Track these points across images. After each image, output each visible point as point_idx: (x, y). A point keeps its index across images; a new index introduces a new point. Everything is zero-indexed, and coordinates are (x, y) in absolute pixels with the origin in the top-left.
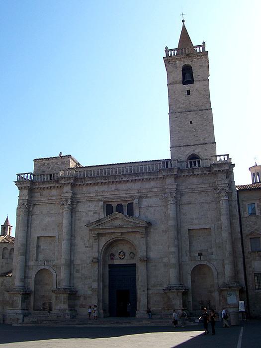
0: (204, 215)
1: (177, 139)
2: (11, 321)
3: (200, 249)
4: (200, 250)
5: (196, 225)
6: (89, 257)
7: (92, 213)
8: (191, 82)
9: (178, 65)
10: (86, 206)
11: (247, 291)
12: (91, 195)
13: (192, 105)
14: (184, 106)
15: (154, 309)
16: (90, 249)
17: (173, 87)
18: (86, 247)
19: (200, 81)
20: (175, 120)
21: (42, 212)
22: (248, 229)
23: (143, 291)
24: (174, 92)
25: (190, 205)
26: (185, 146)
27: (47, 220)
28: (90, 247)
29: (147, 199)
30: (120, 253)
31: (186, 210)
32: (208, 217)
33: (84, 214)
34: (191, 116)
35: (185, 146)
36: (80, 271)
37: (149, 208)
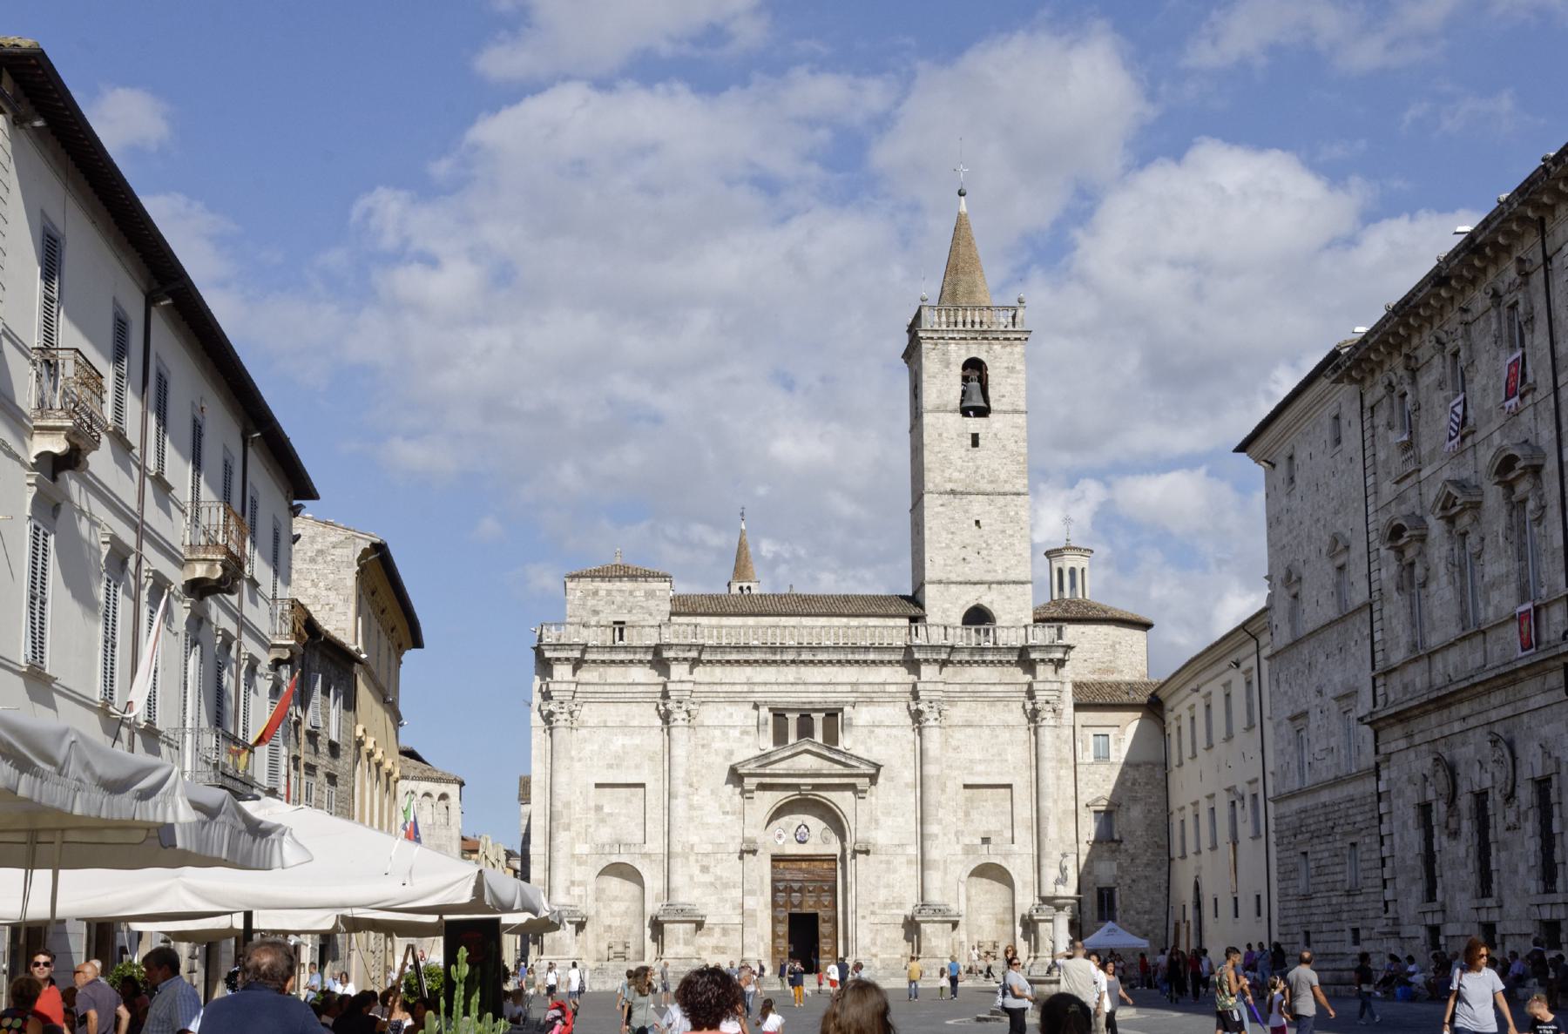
0: (1000, 755)
1: (942, 562)
5: (980, 774)
6: (733, 838)
7: (735, 733)
8: (983, 412)
9: (954, 355)
10: (722, 713)
11: (1080, 926)
12: (738, 688)
13: (983, 477)
14: (963, 476)
15: (885, 956)
16: (734, 817)
17: (938, 418)
18: (724, 813)
19: (1005, 412)
20: (938, 513)
21: (605, 722)
22: (1091, 790)
23: (864, 917)
24: (940, 435)
25: (969, 731)
26: (961, 583)
27: (619, 741)
28: (734, 813)
29: (872, 708)
30: (800, 827)
31: (959, 740)
32: (1006, 761)
33: (717, 733)
34: (978, 506)
35: (961, 583)
37: (876, 730)
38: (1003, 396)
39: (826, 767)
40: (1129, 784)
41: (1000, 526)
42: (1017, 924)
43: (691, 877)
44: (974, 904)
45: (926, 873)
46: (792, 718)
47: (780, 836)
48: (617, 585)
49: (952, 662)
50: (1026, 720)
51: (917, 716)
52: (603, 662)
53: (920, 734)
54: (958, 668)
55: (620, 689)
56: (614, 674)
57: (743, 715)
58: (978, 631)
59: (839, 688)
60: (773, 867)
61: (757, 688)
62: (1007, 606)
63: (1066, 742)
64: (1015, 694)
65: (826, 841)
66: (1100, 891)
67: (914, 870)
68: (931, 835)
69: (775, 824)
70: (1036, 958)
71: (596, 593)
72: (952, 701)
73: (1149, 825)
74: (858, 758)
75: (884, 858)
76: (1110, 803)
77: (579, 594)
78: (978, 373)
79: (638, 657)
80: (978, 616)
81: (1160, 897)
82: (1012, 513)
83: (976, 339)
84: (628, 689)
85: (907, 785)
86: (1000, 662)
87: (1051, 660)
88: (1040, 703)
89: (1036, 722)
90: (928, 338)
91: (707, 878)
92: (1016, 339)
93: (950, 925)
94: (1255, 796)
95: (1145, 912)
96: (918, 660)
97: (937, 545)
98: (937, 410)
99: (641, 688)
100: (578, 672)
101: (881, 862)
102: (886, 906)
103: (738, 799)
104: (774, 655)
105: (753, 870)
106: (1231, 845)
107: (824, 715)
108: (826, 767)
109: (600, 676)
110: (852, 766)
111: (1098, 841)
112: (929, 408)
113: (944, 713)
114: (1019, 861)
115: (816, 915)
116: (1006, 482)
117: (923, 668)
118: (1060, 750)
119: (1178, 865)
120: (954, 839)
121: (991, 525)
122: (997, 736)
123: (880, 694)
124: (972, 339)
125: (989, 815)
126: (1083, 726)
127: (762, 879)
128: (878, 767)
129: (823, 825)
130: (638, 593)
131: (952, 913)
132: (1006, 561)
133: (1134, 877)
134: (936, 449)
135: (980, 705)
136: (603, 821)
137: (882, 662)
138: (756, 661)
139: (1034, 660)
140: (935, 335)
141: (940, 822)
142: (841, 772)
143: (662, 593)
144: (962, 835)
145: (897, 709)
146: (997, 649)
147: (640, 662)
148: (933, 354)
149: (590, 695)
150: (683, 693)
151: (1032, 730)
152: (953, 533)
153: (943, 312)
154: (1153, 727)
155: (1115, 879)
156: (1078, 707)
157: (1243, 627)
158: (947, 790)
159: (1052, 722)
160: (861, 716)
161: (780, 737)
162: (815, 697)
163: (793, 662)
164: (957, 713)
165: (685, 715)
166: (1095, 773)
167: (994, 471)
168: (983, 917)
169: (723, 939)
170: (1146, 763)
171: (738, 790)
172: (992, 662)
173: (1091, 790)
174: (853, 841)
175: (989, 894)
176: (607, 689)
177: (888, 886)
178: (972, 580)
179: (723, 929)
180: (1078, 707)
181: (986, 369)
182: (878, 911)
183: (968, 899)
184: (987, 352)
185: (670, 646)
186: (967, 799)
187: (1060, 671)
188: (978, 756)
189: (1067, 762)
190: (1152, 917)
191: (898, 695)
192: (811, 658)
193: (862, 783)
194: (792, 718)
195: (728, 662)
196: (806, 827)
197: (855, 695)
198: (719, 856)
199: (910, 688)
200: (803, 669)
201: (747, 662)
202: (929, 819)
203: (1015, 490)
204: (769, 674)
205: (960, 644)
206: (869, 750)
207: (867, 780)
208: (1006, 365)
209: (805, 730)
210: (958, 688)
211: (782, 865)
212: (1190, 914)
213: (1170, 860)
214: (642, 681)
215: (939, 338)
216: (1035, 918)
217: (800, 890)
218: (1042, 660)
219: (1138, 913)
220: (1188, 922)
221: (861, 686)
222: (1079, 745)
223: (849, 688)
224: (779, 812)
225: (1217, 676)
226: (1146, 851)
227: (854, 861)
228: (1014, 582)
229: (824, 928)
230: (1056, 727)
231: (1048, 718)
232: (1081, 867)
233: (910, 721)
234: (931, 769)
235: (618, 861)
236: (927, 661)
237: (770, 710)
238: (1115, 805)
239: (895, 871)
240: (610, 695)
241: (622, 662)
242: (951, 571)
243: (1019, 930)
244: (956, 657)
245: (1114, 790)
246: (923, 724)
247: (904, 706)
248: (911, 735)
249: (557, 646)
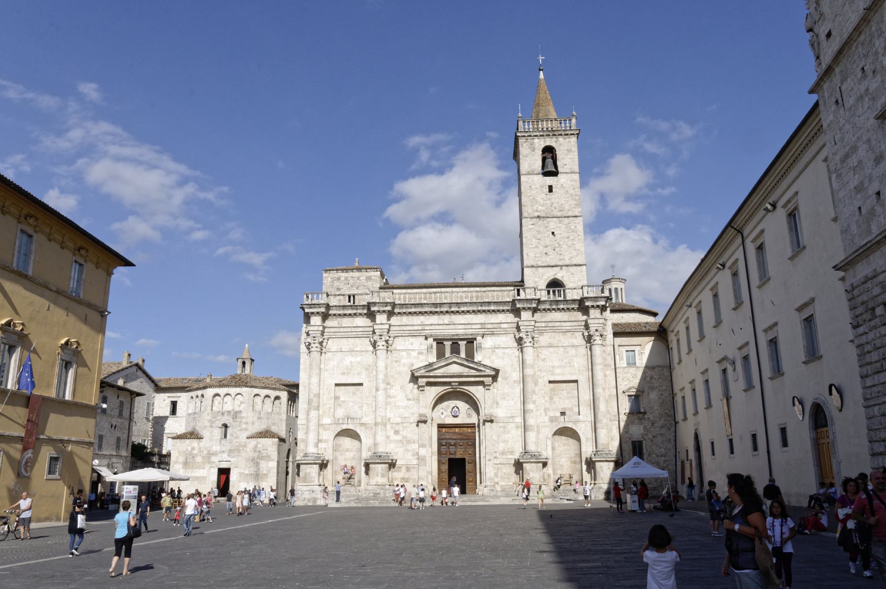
0: (570, 363)
1: (534, 255)
2: (306, 502)
3: (563, 407)
4: (562, 409)
5: (558, 375)
6: (413, 414)
7: (415, 354)
8: (555, 174)
9: (537, 145)
10: (407, 342)
12: (416, 328)
13: (555, 208)
14: (544, 208)
15: (503, 483)
16: (414, 402)
17: (529, 178)
18: (408, 400)
19: (567, 173)
20: (530, 229)
21: (341, 349)
22: (626, 383)
23: (490, 460)
24: (530, 187)
25: (551, 349)
26: (544, 267)
27: (349, 360)
28: (414, 400)
29: (494, 338)
32: (574, 366)
33: (404, 353)
34: (553, 224)
35: (544, 267)
36: (400, 433)
37: (497, 350)
38: (566, 165)
39: (466, 371)
40: (648, 379)
41: (567, 235)
42: (583, 463)
43: (388, 437)
44: (557, 452)
45: (526, 433)
46: (448, 344)
47: (442, 413)
48: (351, 274)
49: (539, 310)
50: (585, 342)
51: (520, 341)
52: (340, 315)
53: (522, 351)
54: (544, 313)
55: (349, 330)
56: (346, 322)
57: (420, 344)
58: (554, 292)
59: (474, 327)
60: (439, 431)
61: (426, 328)
62: (572, 279)
63: (609, 354)
64: (578, 327)
65: (469, 416)
66: (633, 443)
67: (520, 432)
68: (528, 410)
69: (440, 406)
70: (595, 484)
71: (339, 279)
72: (541, 333)
73: (662, 403)
74: (484, 366)
75: (501, 425)
76: (638, 391)
77: (329, 279)
78: (551, 155)
79: (359, 311)
80: (555, 284)
81: (671, 446)
82: (573, 227)
83: (549, 135)
84: (353, 330)
85: (515, 382)
86: (568, 309)
87: (598, 306)
88: (592, 331)
89: (590, 343)
90: (522, 136)
91: (398, 438)
92: (571, 134)
93: (541, 465)
94: (746, 358)
95: (662, 456)
96: (519, 308)
97: (531, 246)
98: (529, 174)
99: (360, 329)
100: (326, 322)
101: (500, 427)
102: (503, 453)
103: (416, 391)
104: (436, 309)
105: (424, 433)
106: (725, 400)
107: (465, 342)
108: (466, 371)
109: (338, 323)
110: (481, 371)
111: (631, 414)
112: (524, 173)
113: (535, 339)
114: (583, 425)
115: (464, 459)
116: (569, 210)
117: (522, 313)
118: (606, 360)
119: (682, 425)
120: (542, 411)
121: (561, 234)
122: (568, 352)
123: (498, 330)
124: (547, 135)
125: (565, 398)
126: (619, 346)
127: (431, 438)
128: (497, 371)
129: (468, 406)
130: (362, 278)
131: (542, 457)
132: (570, 253)
133: (654, 434)
134: (530, 194)
135: (557, 334)
136: (340, 405)
137: (499, 311)
138: (426, 312)
139: (588, 306)
140: (526, 134)
141: (534, 402)
142: (474, 374)
143: (375, 278)
144: (549, 411)
145: (508, 338)
146: (565, 301)
147: (360, 314)
148: (525, 145)
149: (332, 334)
150: (383, 330)
151: (588, 348)
152: (539, 239)
153: (531, 123)
154: (661, 345)
155: (643, 435)
156: (616, 334)
157: (730, 225)
158: (539, 384)
159: (600, 342)
160: (487, 343)
161: (440, 355)
162: (460, 331)
163: (447, 312)
164: (544, 339)
165: (384, 343)
166: (627, 373)
167: (561, 205)
168: (563, 459)
169: (407, 473)
170: (660, 366)
171: (416, 386)
172: (563, 309)
173: (626, 383)
174: (483, 415)
175: (565, 445)
176: (342, 330)
177: (504, 441)
178: (551, 265)
179: (407, 467)
180: (616, 334)
181: (555, 151)
182: (499, 456)
183: (553, 449)
184: (556, 142)
185: (375, 304)
186: (551, 390)
187: (604, 313)
188: (556, 364)
189: (610, 367)
190: (666, 458)
191: (509, 329)
192: (457, 309)
193: (488, 380)
194: (448, 344)
195: (410, 313)
196: (457, 408)
197: (483, 330)
198: (405, 424)
199: (515, 325)
200: (453, 317)
201: (420, 313)
202: (527, 400)
203: (573, 215)
204: (434, 319)
205: (543, 299)
206: (492, 362)
207: (491, 379)
208: (566, 148)
209: (455, 350)
210: (543, 324)
211: (444, 430)
212: (692, 455)
213: (676, 423)
214: (362, 325)
215: (528, 136)
216: (593, 459)
217: (455, 445)
218: (593, 306)
219: (658, 456)
220: (691, 460)
221: (487, 325)
222: (617, 357)
223: (479, 326)
224: (441, 399)
225: (705, 286)
226: (660, 419)
227: (484, 427)
228: (576, 265)
229: (468, 467)
230: (602, 345)
231: (598, 340)
232: (621, 429)
233: (516, 344)
234: (529, 371)
235: (347, 428)
236: (524, 308)
237: (434, 340)
238: (640, 391)
239: (509, 432)
240: (344, 334)
241: (350, 315)
242: (538, 261)
243: (584, 467)
244: (542, 307)
245: (640, 383)
246: (523, 346)
247: (512, 336)
248: (517, 353)
249: (311, 306)
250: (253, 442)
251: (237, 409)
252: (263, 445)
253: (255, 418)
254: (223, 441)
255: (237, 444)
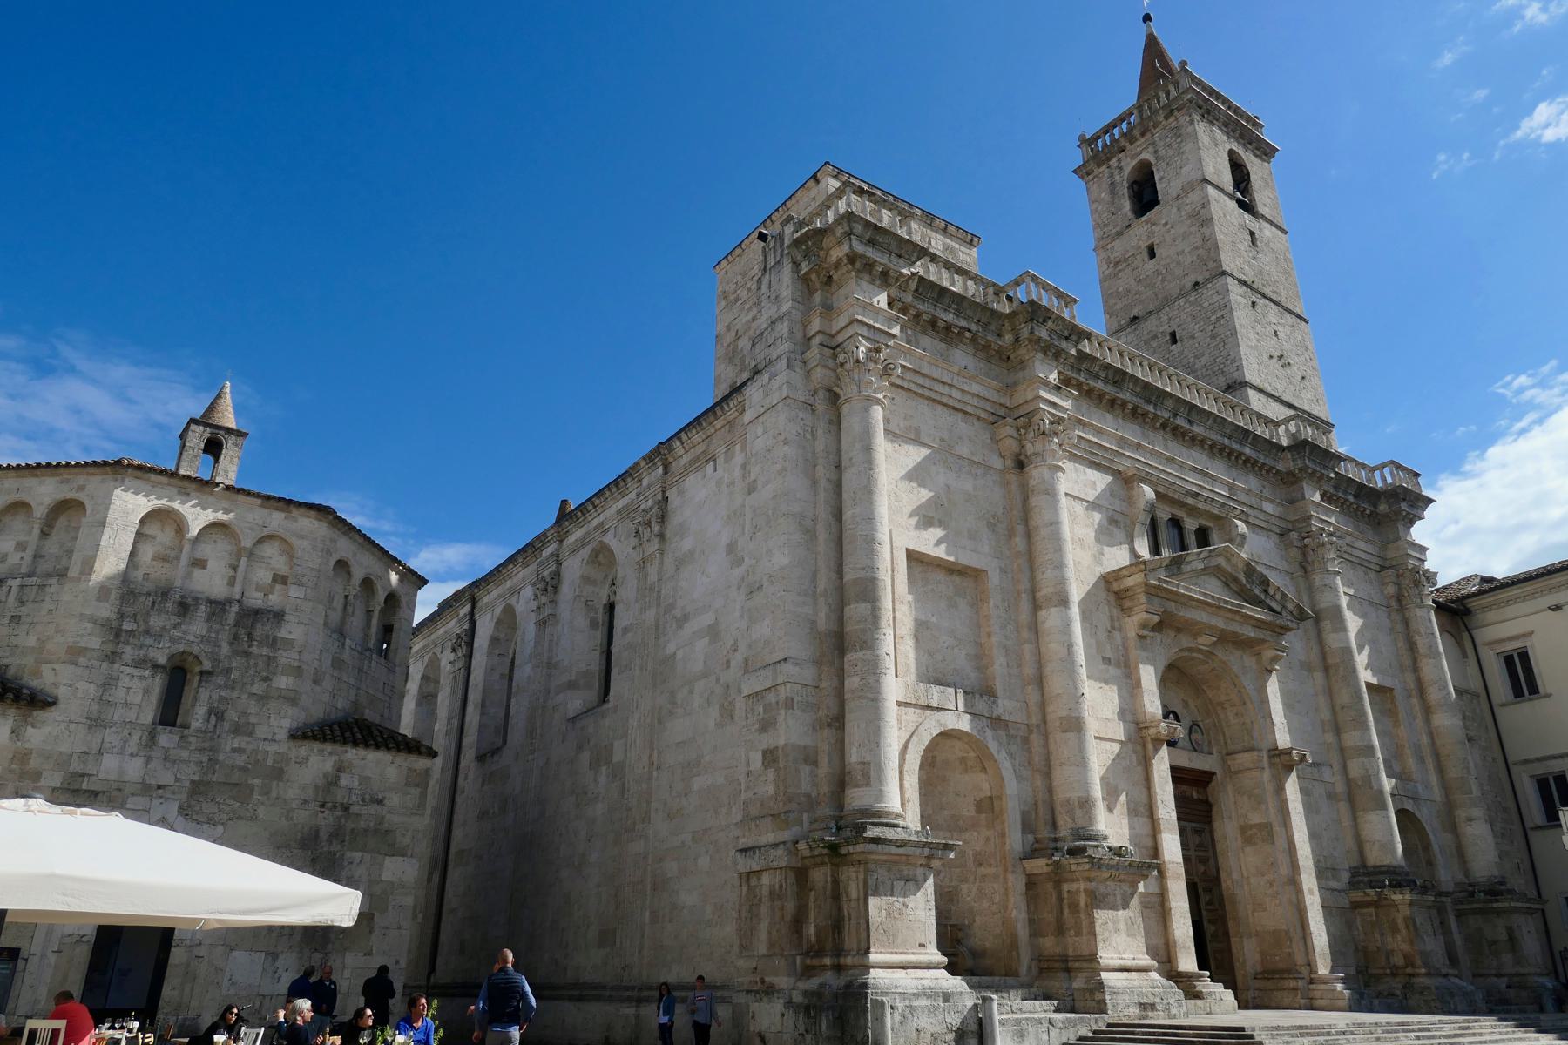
250: (318, 761)
251: (255, 600)
252: (364, 780)
253: (327, 662)
254: (166, 738)
255: (240, 760)
